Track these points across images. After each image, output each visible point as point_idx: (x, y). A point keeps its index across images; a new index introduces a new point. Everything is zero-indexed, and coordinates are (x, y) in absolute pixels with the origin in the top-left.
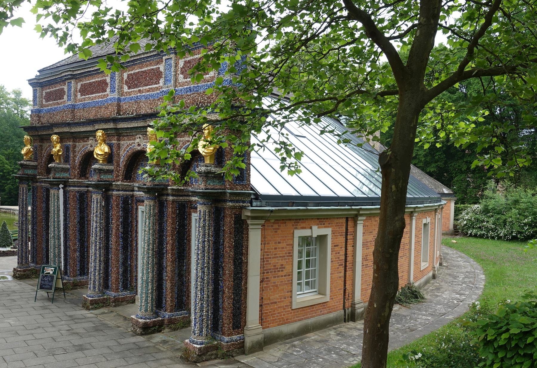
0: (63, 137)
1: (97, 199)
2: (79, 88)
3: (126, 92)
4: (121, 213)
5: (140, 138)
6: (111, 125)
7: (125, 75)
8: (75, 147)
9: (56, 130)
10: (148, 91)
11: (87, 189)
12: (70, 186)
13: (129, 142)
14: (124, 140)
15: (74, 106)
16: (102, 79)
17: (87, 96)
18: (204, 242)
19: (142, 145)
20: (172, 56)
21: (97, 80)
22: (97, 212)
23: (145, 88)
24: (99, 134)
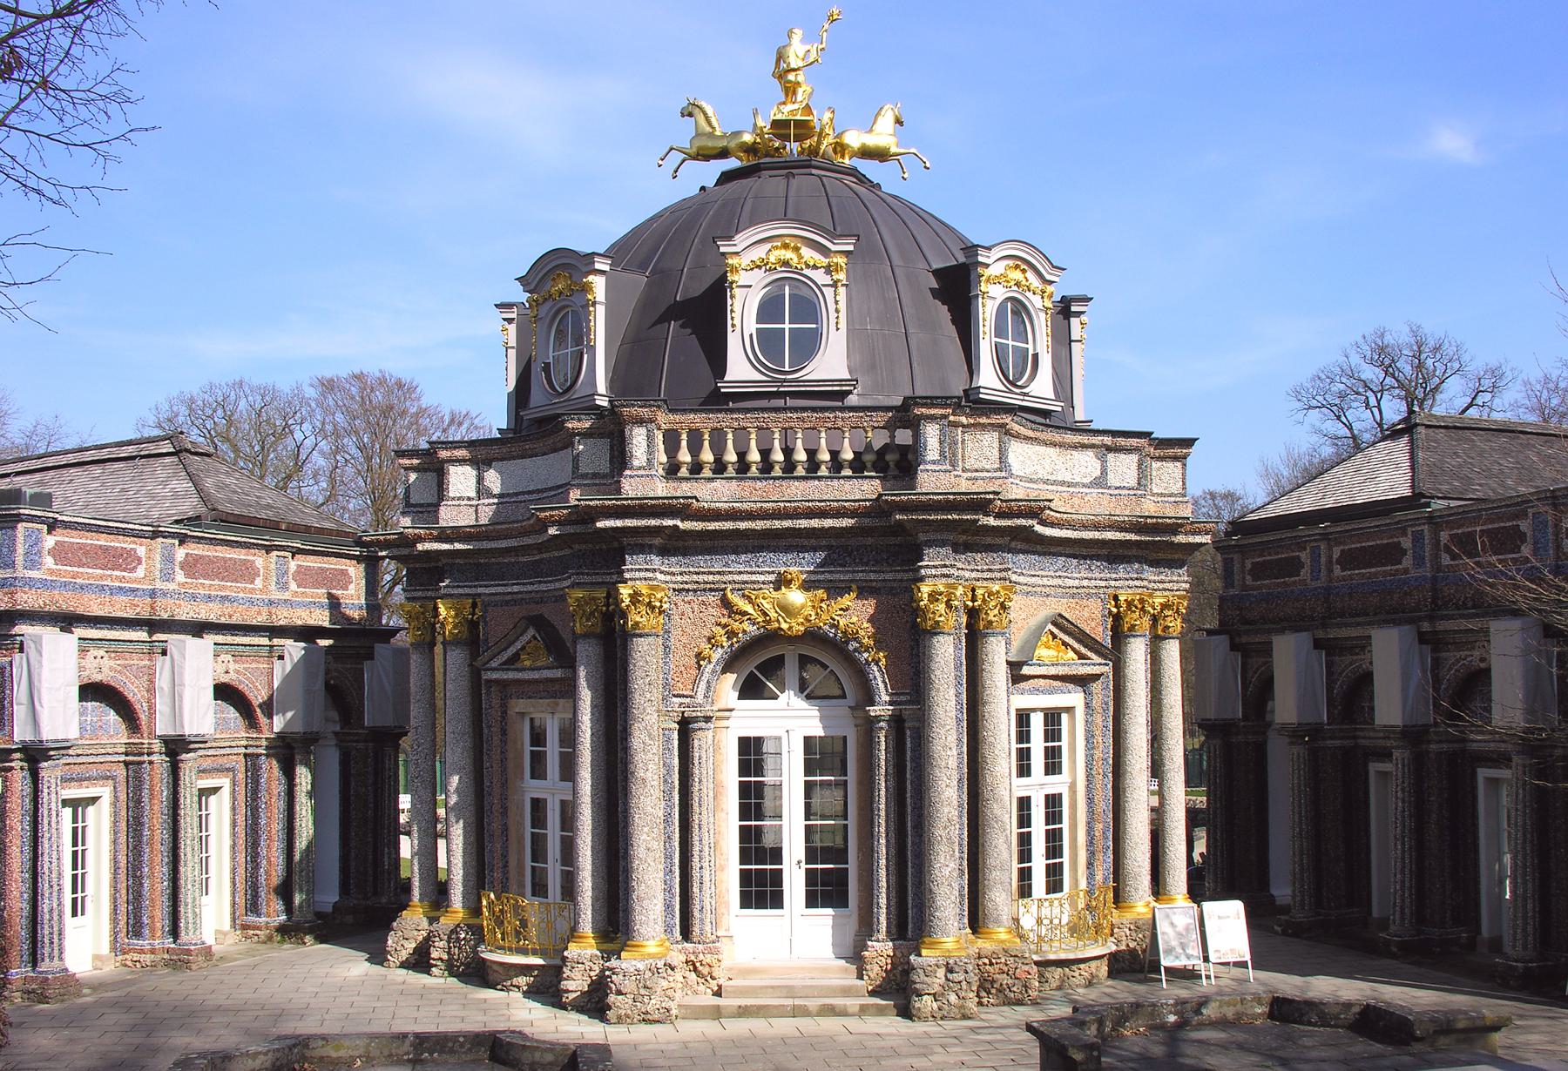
1: (1403, 759)
2: (1335, 557)
4: (1445, 782)
12: (1324, 739)
16: (1391, 541)
17: (1357, 572)
22: (1403, 782)
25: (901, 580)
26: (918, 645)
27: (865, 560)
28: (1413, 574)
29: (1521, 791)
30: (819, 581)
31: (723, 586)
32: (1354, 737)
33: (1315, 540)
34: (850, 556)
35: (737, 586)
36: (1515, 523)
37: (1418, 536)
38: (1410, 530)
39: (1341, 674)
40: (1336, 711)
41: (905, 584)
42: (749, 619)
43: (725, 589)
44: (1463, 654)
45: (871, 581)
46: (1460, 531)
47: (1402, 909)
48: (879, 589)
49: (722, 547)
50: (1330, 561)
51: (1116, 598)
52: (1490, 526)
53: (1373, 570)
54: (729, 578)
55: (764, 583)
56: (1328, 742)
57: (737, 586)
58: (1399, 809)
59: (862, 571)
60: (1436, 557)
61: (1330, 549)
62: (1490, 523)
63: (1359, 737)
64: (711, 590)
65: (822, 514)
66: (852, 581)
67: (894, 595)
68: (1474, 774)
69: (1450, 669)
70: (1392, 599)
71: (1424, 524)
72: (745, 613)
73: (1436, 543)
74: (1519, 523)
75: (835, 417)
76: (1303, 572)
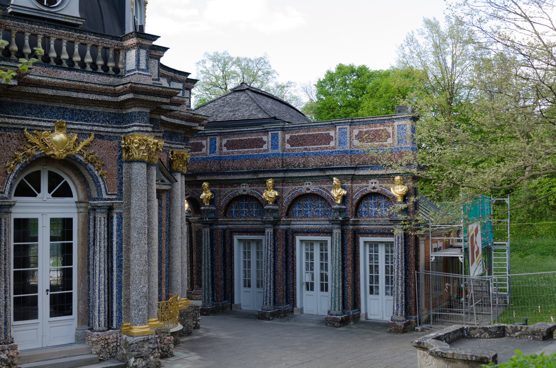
0: (212, 184)
1: (271, 232)
3: (289, 150)
5: (309, 184)
6: (281, 175)
7: (287, 137)
8: (220, 192)
9: (207, 178)
10: (316, 149)
11: (227, 226)
13: (294, 187)
14: (289, 186)
15: (220, 158)
16: (257, 137)
18: (402, 253)
19: (311, 189)
20: (348, 127)
21: (250, 138)
22: (271, 243)
23: (312, 147)
24: (270, 182)
25: (115, 133)
26: (122, 168)
27: (98, 120)
28: (271, 151)
29: (338, 244)
30: (75, 129)
31: (22, 127)
32: (227, 224)
33: (214, 135)
34: (90, 116)
35: (30, 128)
36: (327, 132)
37: (275, 137)
38: (270, 133)
39: (225, 196)
40: (222, 213)
41: (117, 135)
42: (36, 148)
43: (24, 129)
44: (297, 187)
45: (101, 131)
46: (297, 134)
47: (270, 298)
48: (104, 137)
49: (22, 103)
50: (221, 145)
51: (172, 153)
52: (314, 133)
53: (246, 150)
54: (27, 122)
55: (45, 127)
56: (219, 226)
57: (30, 128)
58: (269, 254)
59: (97, 126)
60: (283, 145)
61: (221, 139)
62: (314, 132)
63: (261, 221)
64: (15, 128)
65: (85, 90)
66: (91, 130)
67: (110, 140)
68: (294, 239)
69: (289, 193)
70: (257, 163)
71: (279, 130)
72: (32, 144)
73: (284, 139)
74: (330, 132)
75: (86, 37)
76: (204, 150)
